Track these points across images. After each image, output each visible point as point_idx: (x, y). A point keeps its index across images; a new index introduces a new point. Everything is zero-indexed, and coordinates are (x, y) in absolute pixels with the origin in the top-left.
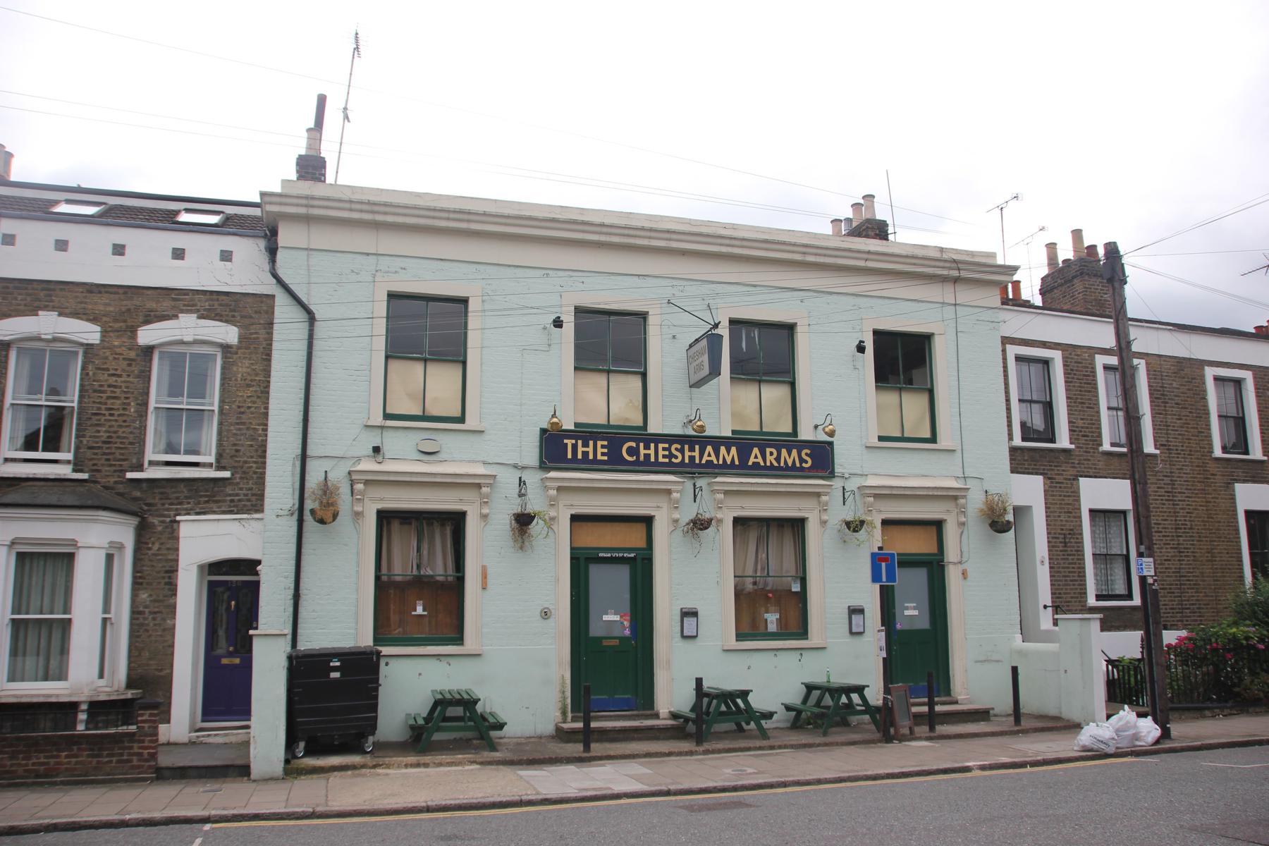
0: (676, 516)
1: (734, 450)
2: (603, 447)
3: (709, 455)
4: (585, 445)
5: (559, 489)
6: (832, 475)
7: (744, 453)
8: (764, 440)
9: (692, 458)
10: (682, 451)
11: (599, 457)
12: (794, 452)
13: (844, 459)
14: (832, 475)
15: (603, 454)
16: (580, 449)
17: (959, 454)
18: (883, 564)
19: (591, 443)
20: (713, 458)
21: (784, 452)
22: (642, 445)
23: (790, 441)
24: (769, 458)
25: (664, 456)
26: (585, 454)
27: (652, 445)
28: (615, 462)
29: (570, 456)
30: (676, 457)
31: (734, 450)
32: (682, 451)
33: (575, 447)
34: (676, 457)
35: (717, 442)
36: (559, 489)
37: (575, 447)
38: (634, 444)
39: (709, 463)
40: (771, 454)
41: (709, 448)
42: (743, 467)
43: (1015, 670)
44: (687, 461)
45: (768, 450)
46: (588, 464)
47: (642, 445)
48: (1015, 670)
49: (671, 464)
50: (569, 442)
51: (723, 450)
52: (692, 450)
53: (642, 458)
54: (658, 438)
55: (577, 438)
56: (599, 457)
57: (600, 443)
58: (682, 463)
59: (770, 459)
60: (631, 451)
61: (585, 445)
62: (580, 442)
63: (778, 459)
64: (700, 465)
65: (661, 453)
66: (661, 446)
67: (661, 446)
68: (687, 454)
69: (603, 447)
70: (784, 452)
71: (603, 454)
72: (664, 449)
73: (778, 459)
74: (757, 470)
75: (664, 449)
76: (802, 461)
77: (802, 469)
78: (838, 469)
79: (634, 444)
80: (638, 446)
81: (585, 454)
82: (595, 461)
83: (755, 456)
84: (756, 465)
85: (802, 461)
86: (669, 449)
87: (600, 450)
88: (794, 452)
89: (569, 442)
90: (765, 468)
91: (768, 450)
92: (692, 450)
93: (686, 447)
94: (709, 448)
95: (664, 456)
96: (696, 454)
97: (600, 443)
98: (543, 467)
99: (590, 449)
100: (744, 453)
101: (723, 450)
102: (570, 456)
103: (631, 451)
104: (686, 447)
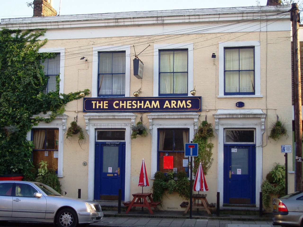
0: (64, 128)
1: (158, 102)
2: (106, 103)
3: (147, 105)
4: (100, 103)
5: (89, 119)
6: (200, 111)
7: (162, 103)
8: (171, 97)
9: (140, 106)
10: (137, 103)
11: (105, 107)
12: (184, 102)
13: (206, 104)
14: (200, 111)
15: (106, 106)
16: (98, 105)
17: (264, 99)
18: (191, 149)
19: (102, 102)
20: (149, 106)
21: (179, 102)
22: (121, 102)
23: (183, 97)
24: (172, 105)
25: (129, 106)
26: (100, 106)
27: (125, 102)
28: (111, 109)
29: (94, 107)
30: (134, 106)
31: (158, 102)
32: (137, 103)
33: (96, 104)
34: (134, 106)
35: (151, 100)
36: (89, 119)
37: (96, 104)
38: (118, 102)
39: (147, 108)
40: (174, 103)
41: (148, 102)
42: (162, 109)
43: (80, 190)
44: (138, 107)
45: (172, 102)
46: (101, 110)
47: (121, 102)
48: (80, 190)
49: (132, 109)
50: (94, 102)
51: (153, 102)
52: (141, 103)
53: (121, 107)
54: (127, 99)
55: (96, 101)
56: (105, 107)
57: (105, 102)
58: (137, 108)
59: (173, 105)
60: (117, 105)
61: (100, 103)
62: (98, 102)
63: (176, 105)
64: (144, 109)
65: (128, 104)
66: (128, 102)
67: (128, 102)
68: (139, 104)
69: (106, 103)
70: (179, 102)
71: (106, 106)
72: (130, 103)
73: (176, 105)
74: (168, 110)
75: (130, 103)
76: (187, 105)
77: (187, 108)
78: (204, 108)
79: (118, 102)
80: (119, 102)
81: (100, 106)
82: (103, 108)
83: (167, 104)
84: (167, 108)
85: (187, 105)
86: (131, 103)
87: (105, 105)
88: (184, 102)
89: (94, 102)
90: (171, 108)
91: (172, 102)
92: (141, 103)
93: (138, 102)
94: (148, 102)
95: (129, 106)
96: (142, 104)
97: (105, 102)
98: (84, 111)
99: (101, 105)
100: (162, 103)
101: (153, 102)
102: (94, 107)
103: (117, 105)
104: (138, 102)
